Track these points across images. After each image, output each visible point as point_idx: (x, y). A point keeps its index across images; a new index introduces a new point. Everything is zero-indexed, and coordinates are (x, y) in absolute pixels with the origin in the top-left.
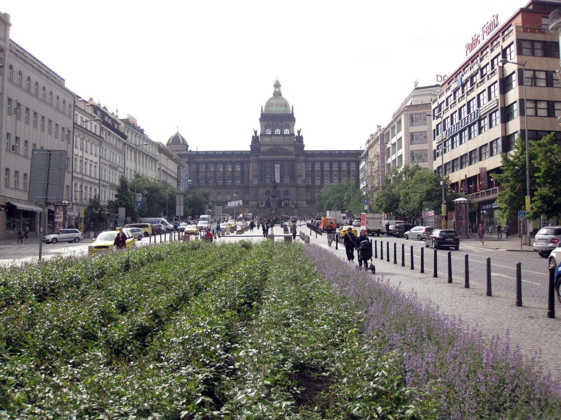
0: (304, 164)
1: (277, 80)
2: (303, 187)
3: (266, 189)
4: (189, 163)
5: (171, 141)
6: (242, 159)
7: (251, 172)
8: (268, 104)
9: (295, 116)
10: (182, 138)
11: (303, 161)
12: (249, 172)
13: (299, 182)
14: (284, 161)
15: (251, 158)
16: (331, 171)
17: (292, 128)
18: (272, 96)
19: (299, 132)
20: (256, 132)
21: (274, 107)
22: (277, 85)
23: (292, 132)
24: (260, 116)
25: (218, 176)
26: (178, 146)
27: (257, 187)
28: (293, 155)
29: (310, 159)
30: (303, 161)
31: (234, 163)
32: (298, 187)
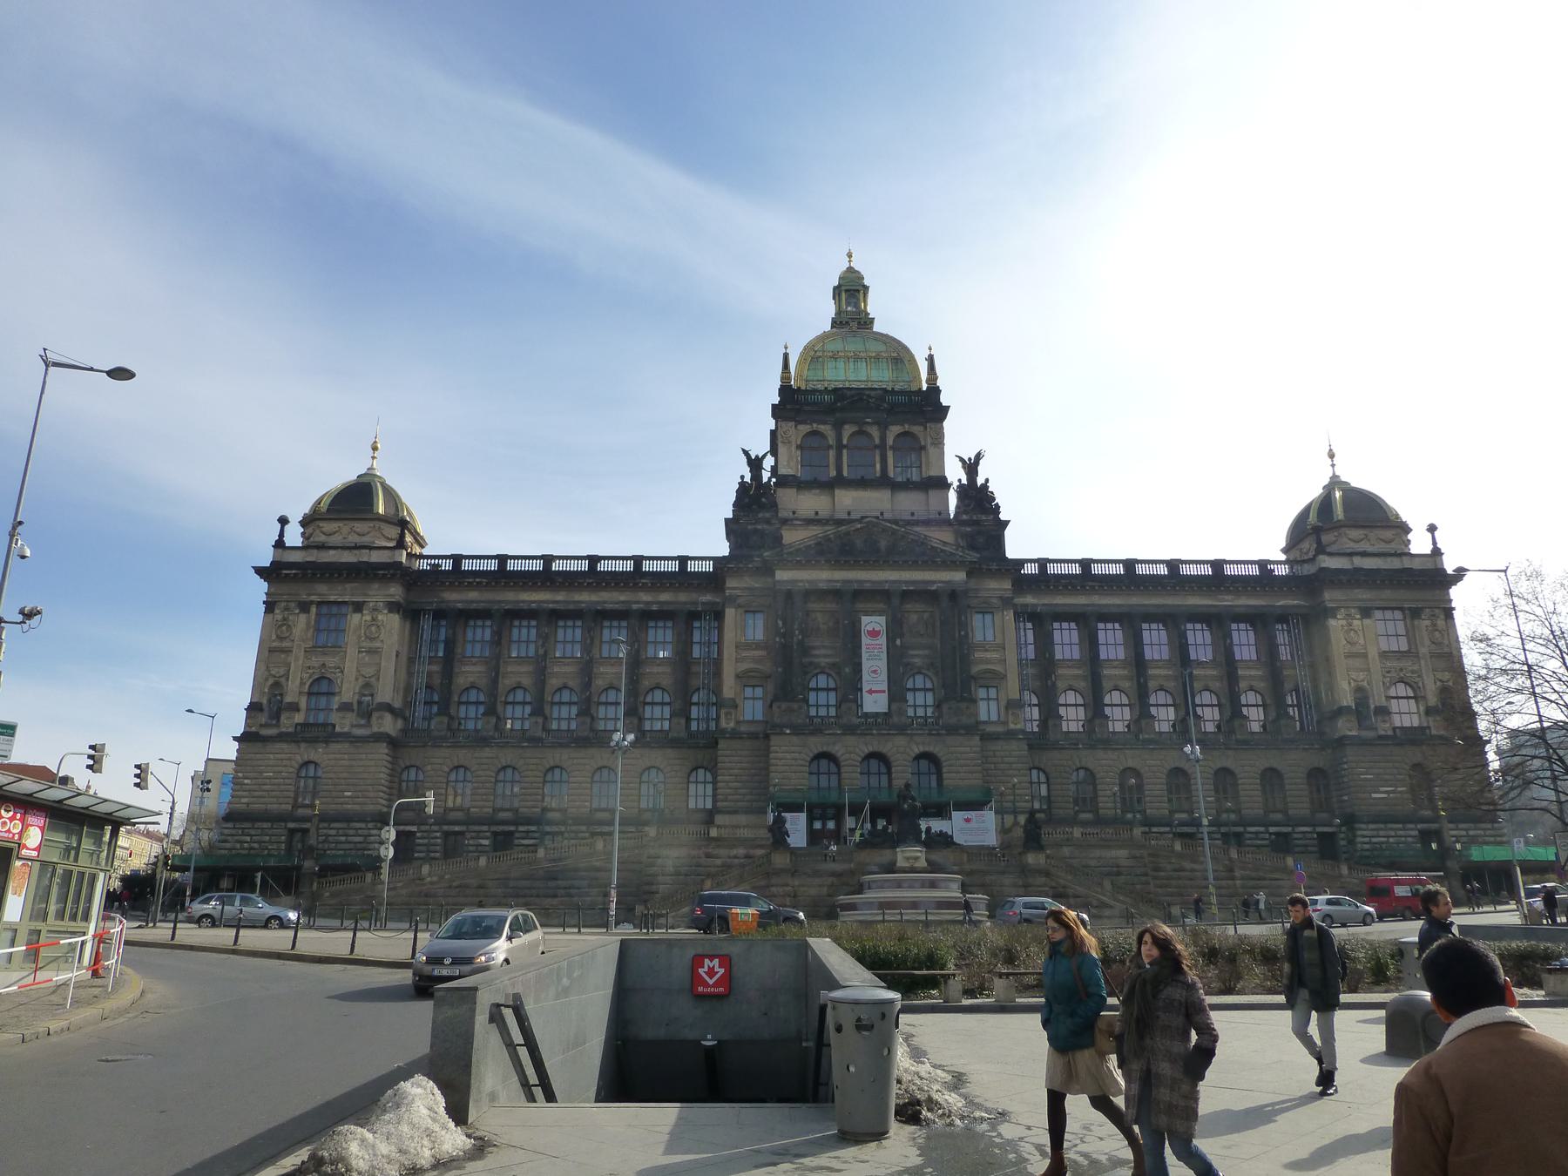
0: (1009, 615)
1: (850, 270)
2: (1010, 735)
3: (816, 744)
4: (411, 613)
5: (324, 506)
6: (683, 597)
7: (729, 653)
8: (815, 354)
9: (944, 400)
10: (391, 495)
11: (1006, 602)
12: (718, 663)
13: (988, 711)
14: (907, 595)
15: (731, 583)
16: (1138, 663)
17: (932, 450)
18: (828, 328)
19: (971, 467)
20: (755, 464)
21: (841, 364)
22: (851, 289)
23: (932, 473)
24: (776, 400)
25: (554, 682)
26: (360, 526)
27: (762, 735)
28: (950, 564)
29: (1029, 600)
30: (1006, 602)
31: (649, 616)
32: (987, 738)
